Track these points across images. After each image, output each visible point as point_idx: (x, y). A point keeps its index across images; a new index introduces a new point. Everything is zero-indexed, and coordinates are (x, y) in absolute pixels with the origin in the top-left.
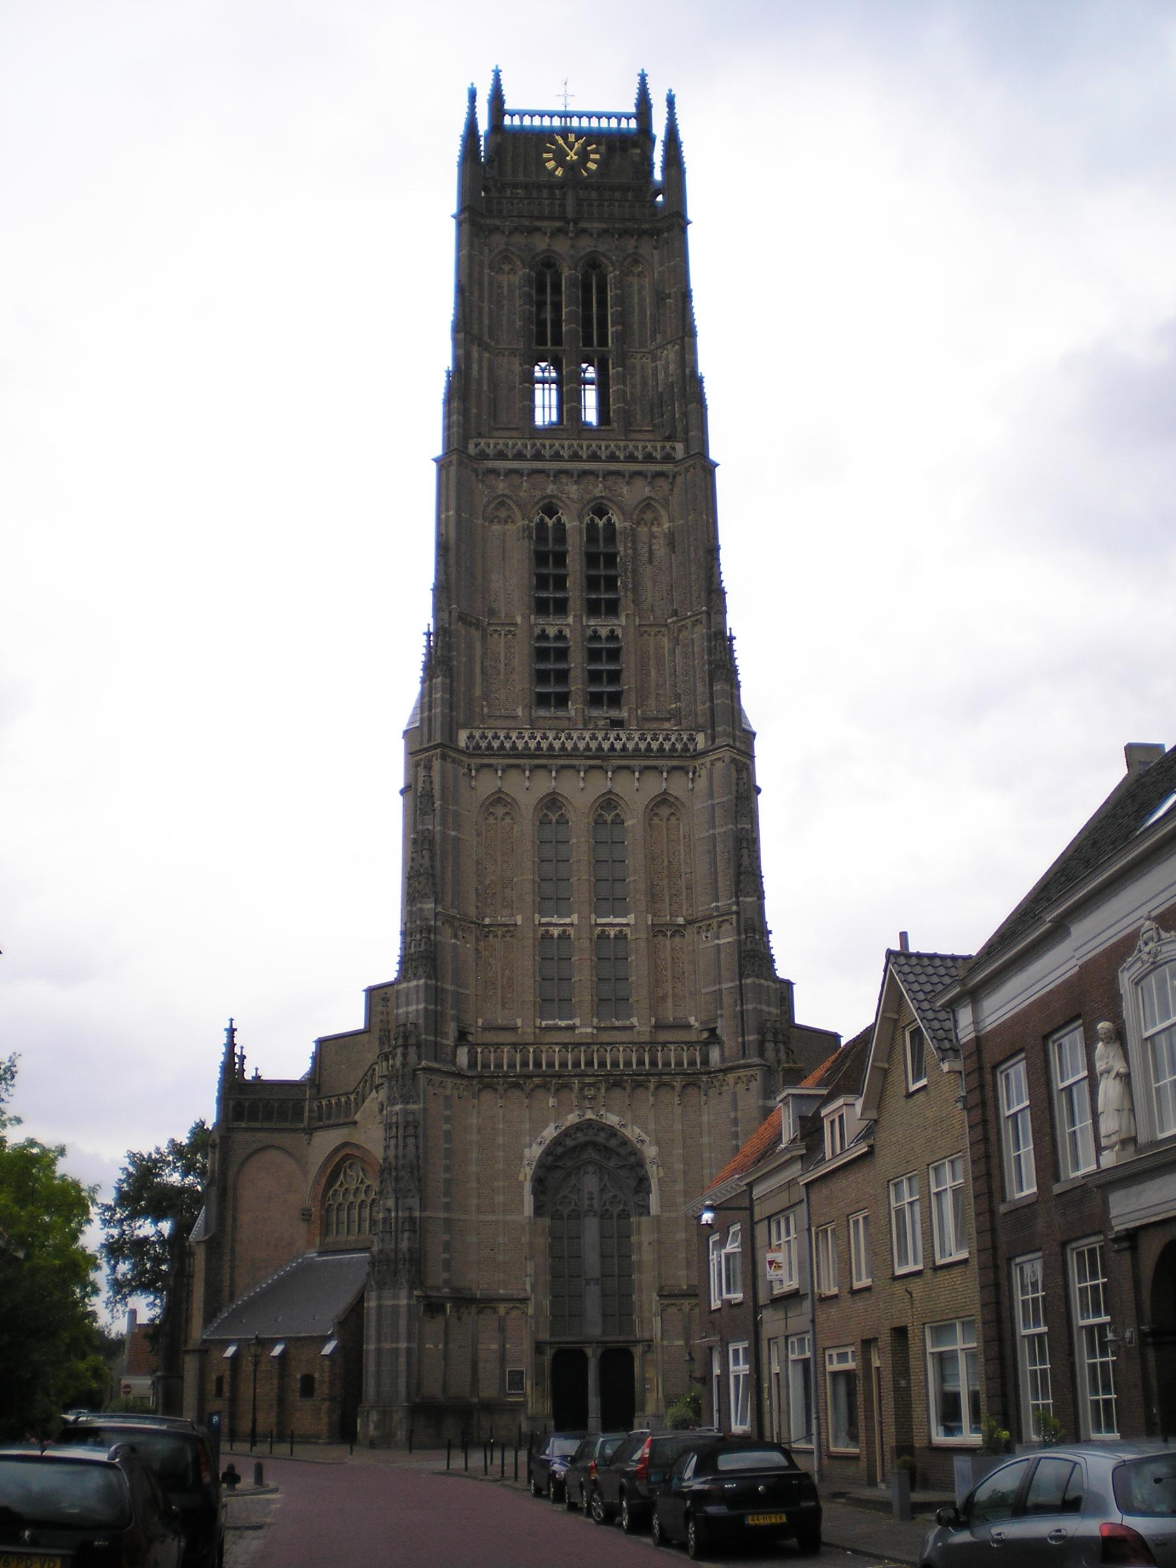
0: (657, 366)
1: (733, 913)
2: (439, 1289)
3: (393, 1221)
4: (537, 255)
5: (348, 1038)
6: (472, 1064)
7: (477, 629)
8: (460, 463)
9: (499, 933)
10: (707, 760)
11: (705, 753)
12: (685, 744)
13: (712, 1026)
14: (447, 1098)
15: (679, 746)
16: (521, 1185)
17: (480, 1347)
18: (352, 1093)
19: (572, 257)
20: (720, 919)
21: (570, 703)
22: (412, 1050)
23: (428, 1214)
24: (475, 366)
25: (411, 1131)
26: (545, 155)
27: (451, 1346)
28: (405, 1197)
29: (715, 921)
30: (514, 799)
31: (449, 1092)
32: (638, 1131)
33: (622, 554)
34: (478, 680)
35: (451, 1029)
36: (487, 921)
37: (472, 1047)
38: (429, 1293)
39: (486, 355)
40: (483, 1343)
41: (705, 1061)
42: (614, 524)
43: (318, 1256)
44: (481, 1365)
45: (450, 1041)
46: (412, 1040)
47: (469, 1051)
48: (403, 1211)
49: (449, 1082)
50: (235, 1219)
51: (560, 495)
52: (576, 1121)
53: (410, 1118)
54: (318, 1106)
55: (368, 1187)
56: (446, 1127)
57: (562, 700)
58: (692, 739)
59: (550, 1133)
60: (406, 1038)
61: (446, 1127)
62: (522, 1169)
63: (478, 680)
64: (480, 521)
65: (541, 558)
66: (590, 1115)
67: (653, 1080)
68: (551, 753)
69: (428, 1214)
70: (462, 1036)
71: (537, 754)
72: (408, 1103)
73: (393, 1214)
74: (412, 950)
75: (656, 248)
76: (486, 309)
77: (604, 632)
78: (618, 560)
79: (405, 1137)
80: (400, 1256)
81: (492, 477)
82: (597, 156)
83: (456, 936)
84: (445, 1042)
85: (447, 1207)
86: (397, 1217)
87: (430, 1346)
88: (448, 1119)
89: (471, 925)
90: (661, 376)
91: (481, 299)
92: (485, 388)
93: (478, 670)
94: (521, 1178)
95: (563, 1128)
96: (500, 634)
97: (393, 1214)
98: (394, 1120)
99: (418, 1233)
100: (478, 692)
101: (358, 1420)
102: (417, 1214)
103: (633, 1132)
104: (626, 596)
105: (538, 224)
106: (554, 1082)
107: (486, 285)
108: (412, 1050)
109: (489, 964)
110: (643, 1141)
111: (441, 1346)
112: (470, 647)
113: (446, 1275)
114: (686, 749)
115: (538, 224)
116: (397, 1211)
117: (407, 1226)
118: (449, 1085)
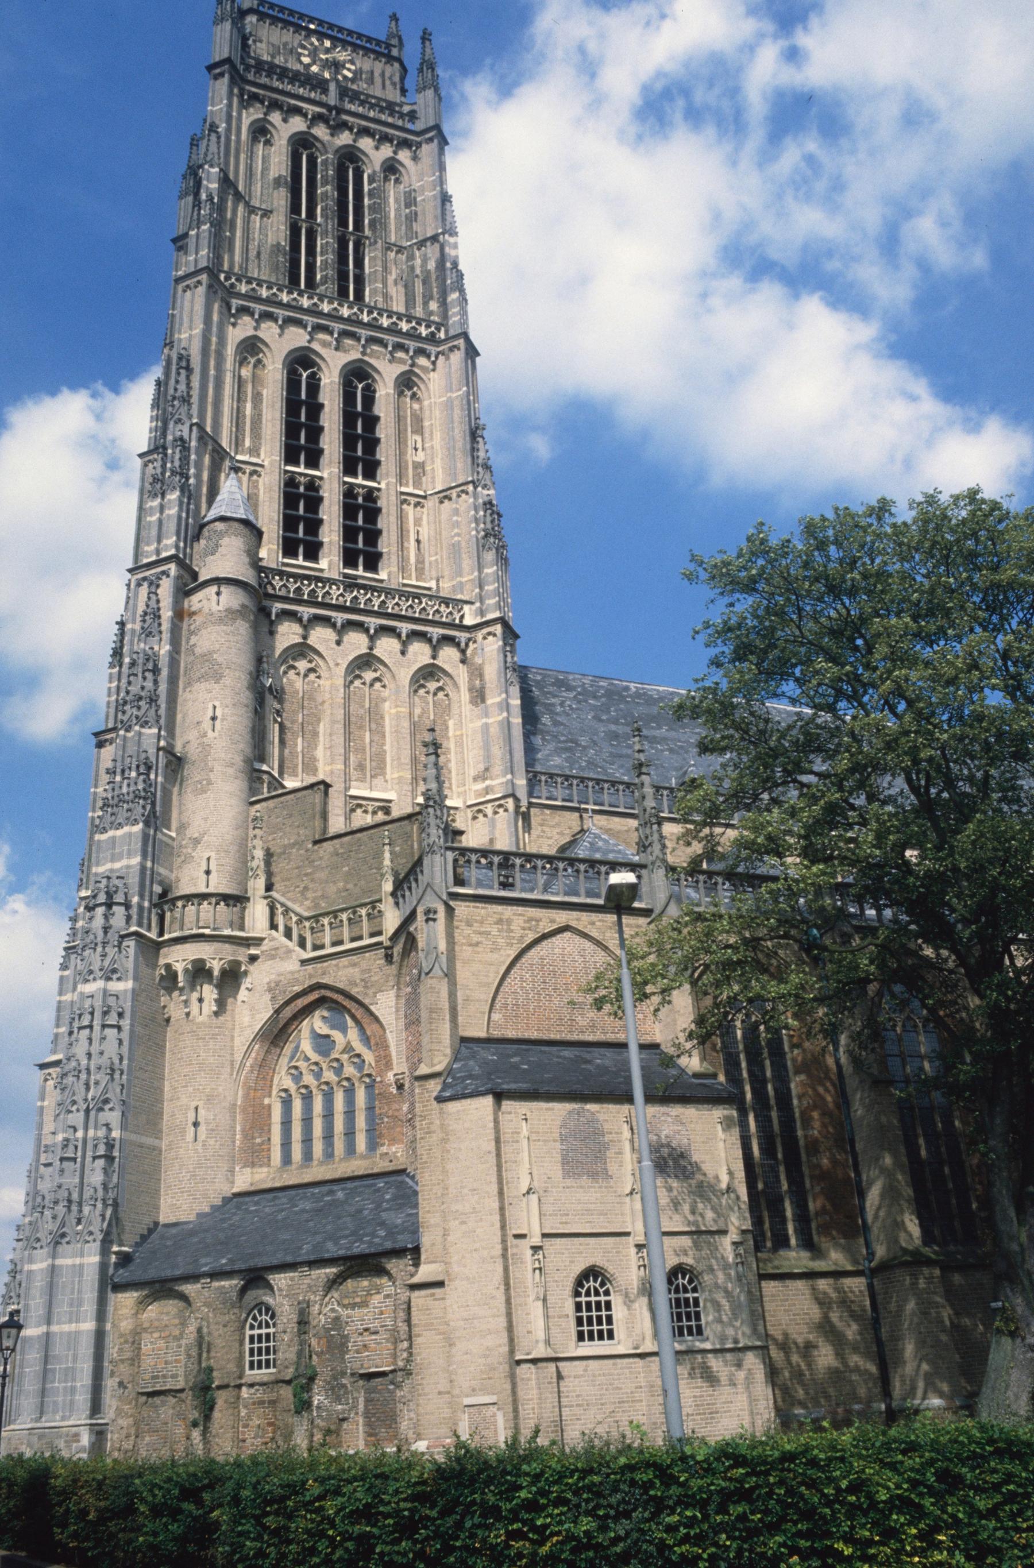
3: (80, 1145)
8: (210, 287)
22: (119, 911)
25: (113, 1019)
28: (101, 1109)
46: (119, 898)
48: (96, 1128)
53: (111, 1002)
60: (109, 895)
72: (109, 979)
73: (80, 1134)
74: (125, 790)
79: (104, 1026)
80: (88, 1193)
86: (85, 1140)
97: (80, 1134)
98: (88, 1003)
102: (116, 1134)
108: (119, 911)
116: (86, 1129)
117: (102, 1150)
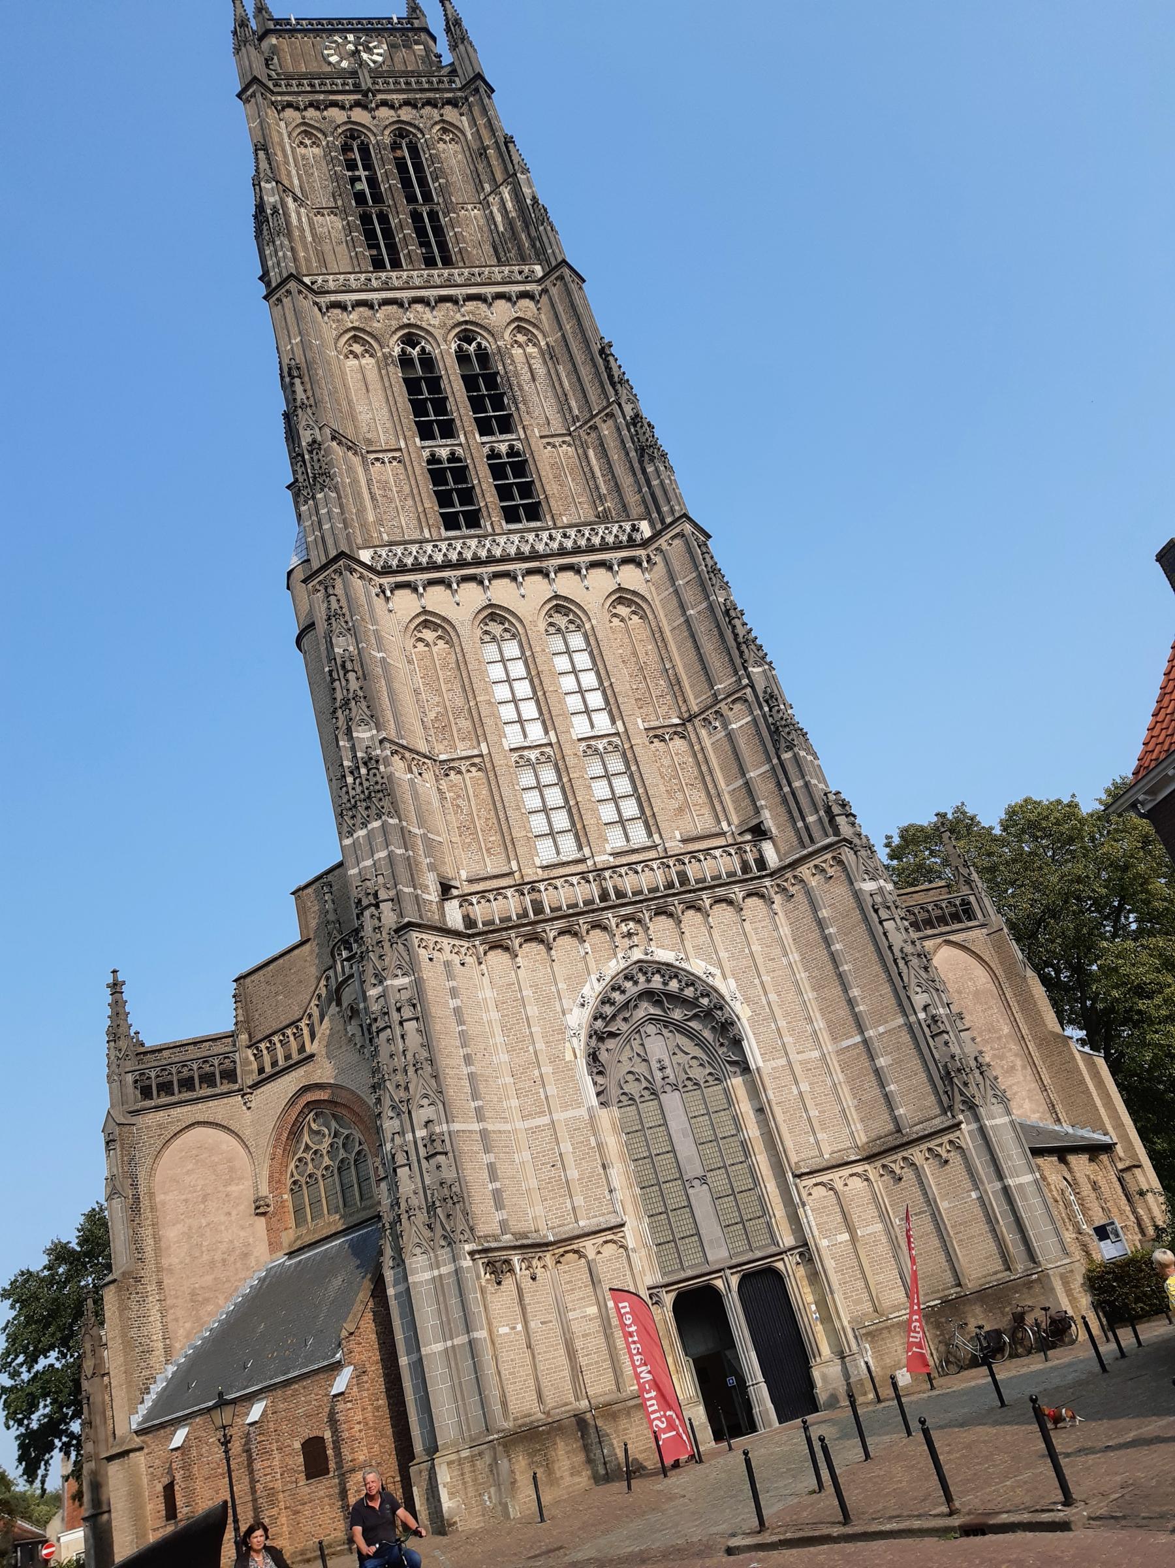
0: (491, 212)
1: (745, 687)
2: (496, 1238)
4: (339, 126)
5: (281, 961)
6: (469, 922)
7: (355, 453)
9: (463, 769)
10: (662, 542)
11: (656, 535)
12: (630, 536)
13: (755, 822)
14: (447, 964)
15: (625, 538)
16: (570, 1068)
17: (571, 1315)
18: (300, 1020)
19: (376, 126)
20: (729, 700)
21: (482, 522)
23: (456, 1126)
24: (294, 216)
26: (326, 52)
27: (532, 1325)
29: (722, 705)
30: (444, 619)
31: (447, 955)
32: (703, 964)
33: (502, 372)
34: (368, 503)
35: (431, 881)
36: (443, 757)
37: (464, 899)
38: (486, 1245)
39: (302, 210)
40: (575, 1310)
41: (761, 863)
42: (485, 348)
43: (289, 1259)
44: (579, 1344)
45: (433, 895)
47: (461, 906)
49: (446, 942)
50: (157, 1239)
51: (419, 323)
52: (622, 967)
54: (255, 1055)
55: (347, 1137)
56: (453, 1003)
57: (473, 520)
58: (635, 529)
59: (592, 990)
61: (453, 1003)
62: (567, 1044)
63: (368, 503)
64: (334, 353)
65: (412, 386)
66: (637, 955)
67: (704, 897)
68: (477, 562)
69: (456, 1126)
70: (446, 889)
71: (462, 564)
75: (462, 115)
76: (294, 172)
77: (503, 448)
78: (499, 380)
81: (338, 311)
82: (381, 51)
83: (411, 771)
84: (426, 896)
85: (480, 1115)
87: (504, 1330)
88: (454, 993)
89: (426, 761)
90: (499, 218)
91: (287, 163)
92: (310, 239)
93: (366, 496)
94: (569, 1056)
95: (608, 979)
96: (383, 463)
99: (450, 1155)
100: (371, 517)
101: (415, 1489)
103: (697, 966)
104: (518, 409)
105: (332, 97)
106: (581, 922)
107: (289, 152)
109: (458, 806)
110: (713, 976)
111: (519, 1327)
112: (350, 469)
113: (499, 1216)
114: (630, 538)
115: (332, 97)
118: (447, 948)
